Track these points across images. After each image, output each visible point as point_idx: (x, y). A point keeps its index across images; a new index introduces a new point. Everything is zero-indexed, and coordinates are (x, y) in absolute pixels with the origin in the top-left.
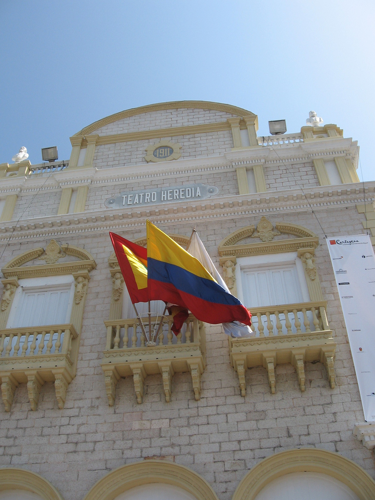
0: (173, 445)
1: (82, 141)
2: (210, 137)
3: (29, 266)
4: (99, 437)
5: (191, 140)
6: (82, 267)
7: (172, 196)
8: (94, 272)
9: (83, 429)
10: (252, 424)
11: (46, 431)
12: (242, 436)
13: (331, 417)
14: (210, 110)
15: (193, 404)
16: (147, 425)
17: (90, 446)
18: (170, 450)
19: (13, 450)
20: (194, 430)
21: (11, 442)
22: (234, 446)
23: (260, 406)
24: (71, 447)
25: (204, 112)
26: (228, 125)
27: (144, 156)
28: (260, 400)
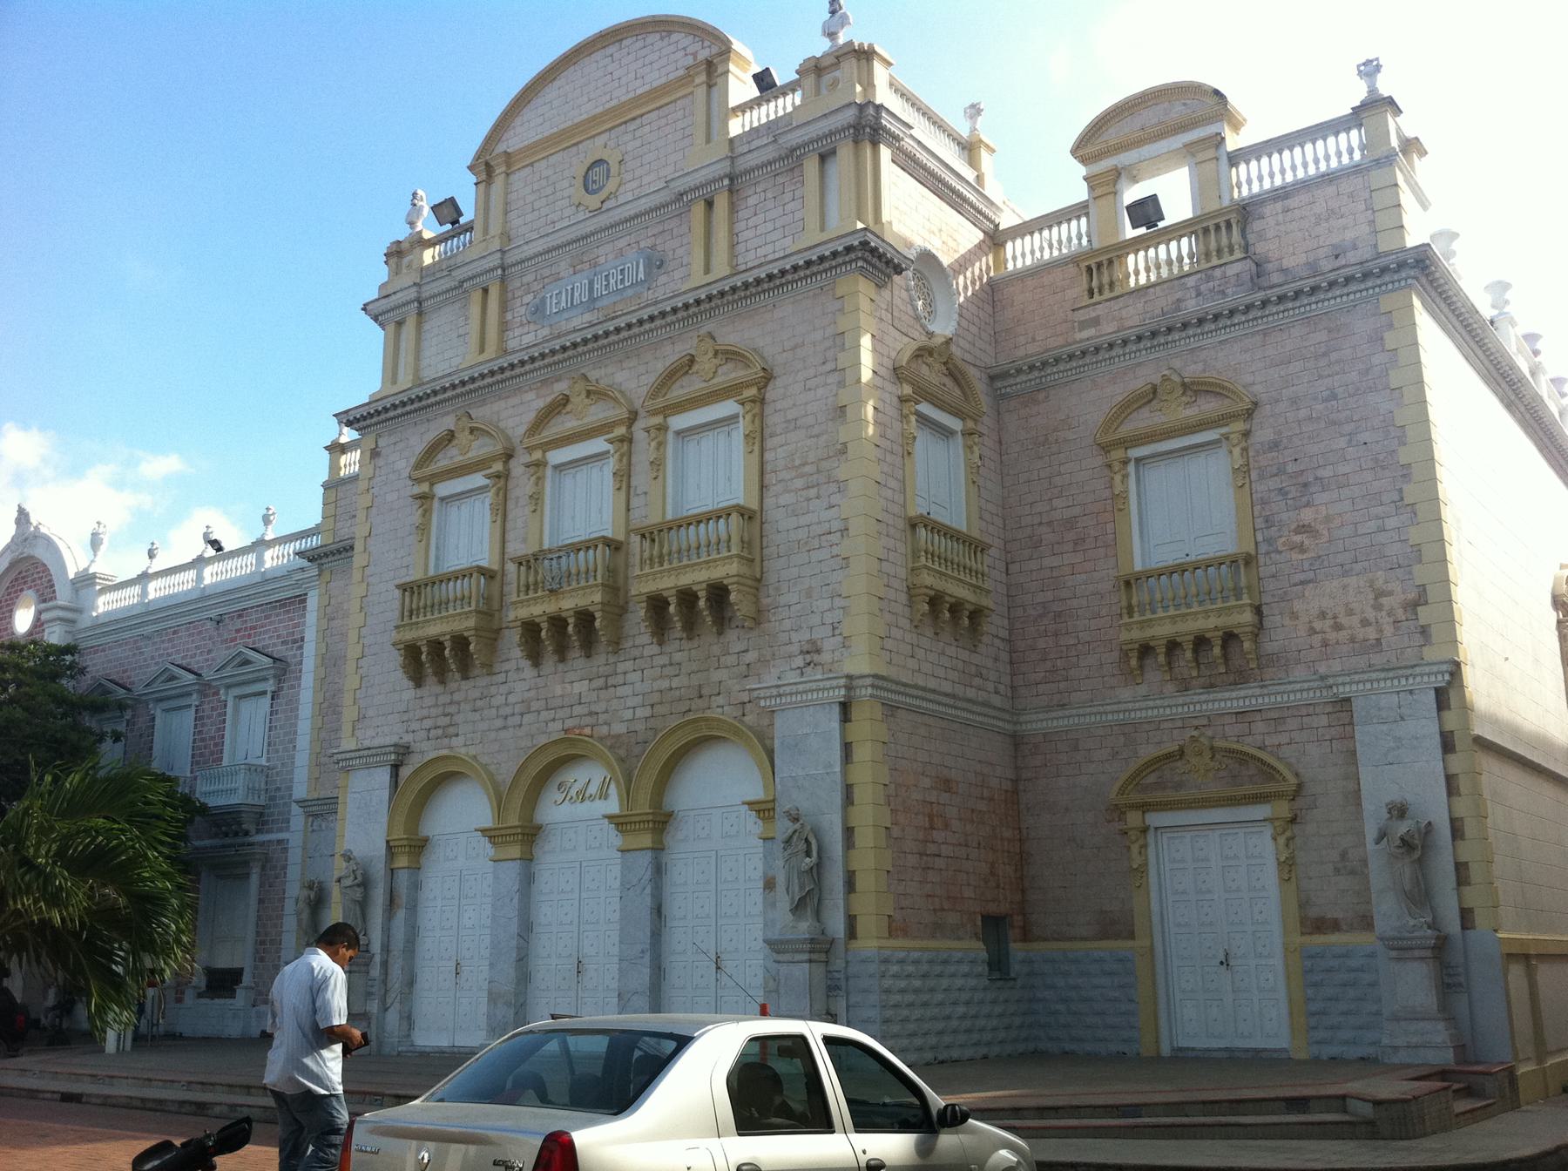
0: (591, 714)
1: (485, 167)
6: (493, 459)
8: (513, 463)
9: (511, 699)
14: (670, 33)
17: (517, 719)
18: (588, 720)
19: (451, 730)
21: (446, 720)
23: (678, 657)
25: (659, 44)
26: (687, 78)
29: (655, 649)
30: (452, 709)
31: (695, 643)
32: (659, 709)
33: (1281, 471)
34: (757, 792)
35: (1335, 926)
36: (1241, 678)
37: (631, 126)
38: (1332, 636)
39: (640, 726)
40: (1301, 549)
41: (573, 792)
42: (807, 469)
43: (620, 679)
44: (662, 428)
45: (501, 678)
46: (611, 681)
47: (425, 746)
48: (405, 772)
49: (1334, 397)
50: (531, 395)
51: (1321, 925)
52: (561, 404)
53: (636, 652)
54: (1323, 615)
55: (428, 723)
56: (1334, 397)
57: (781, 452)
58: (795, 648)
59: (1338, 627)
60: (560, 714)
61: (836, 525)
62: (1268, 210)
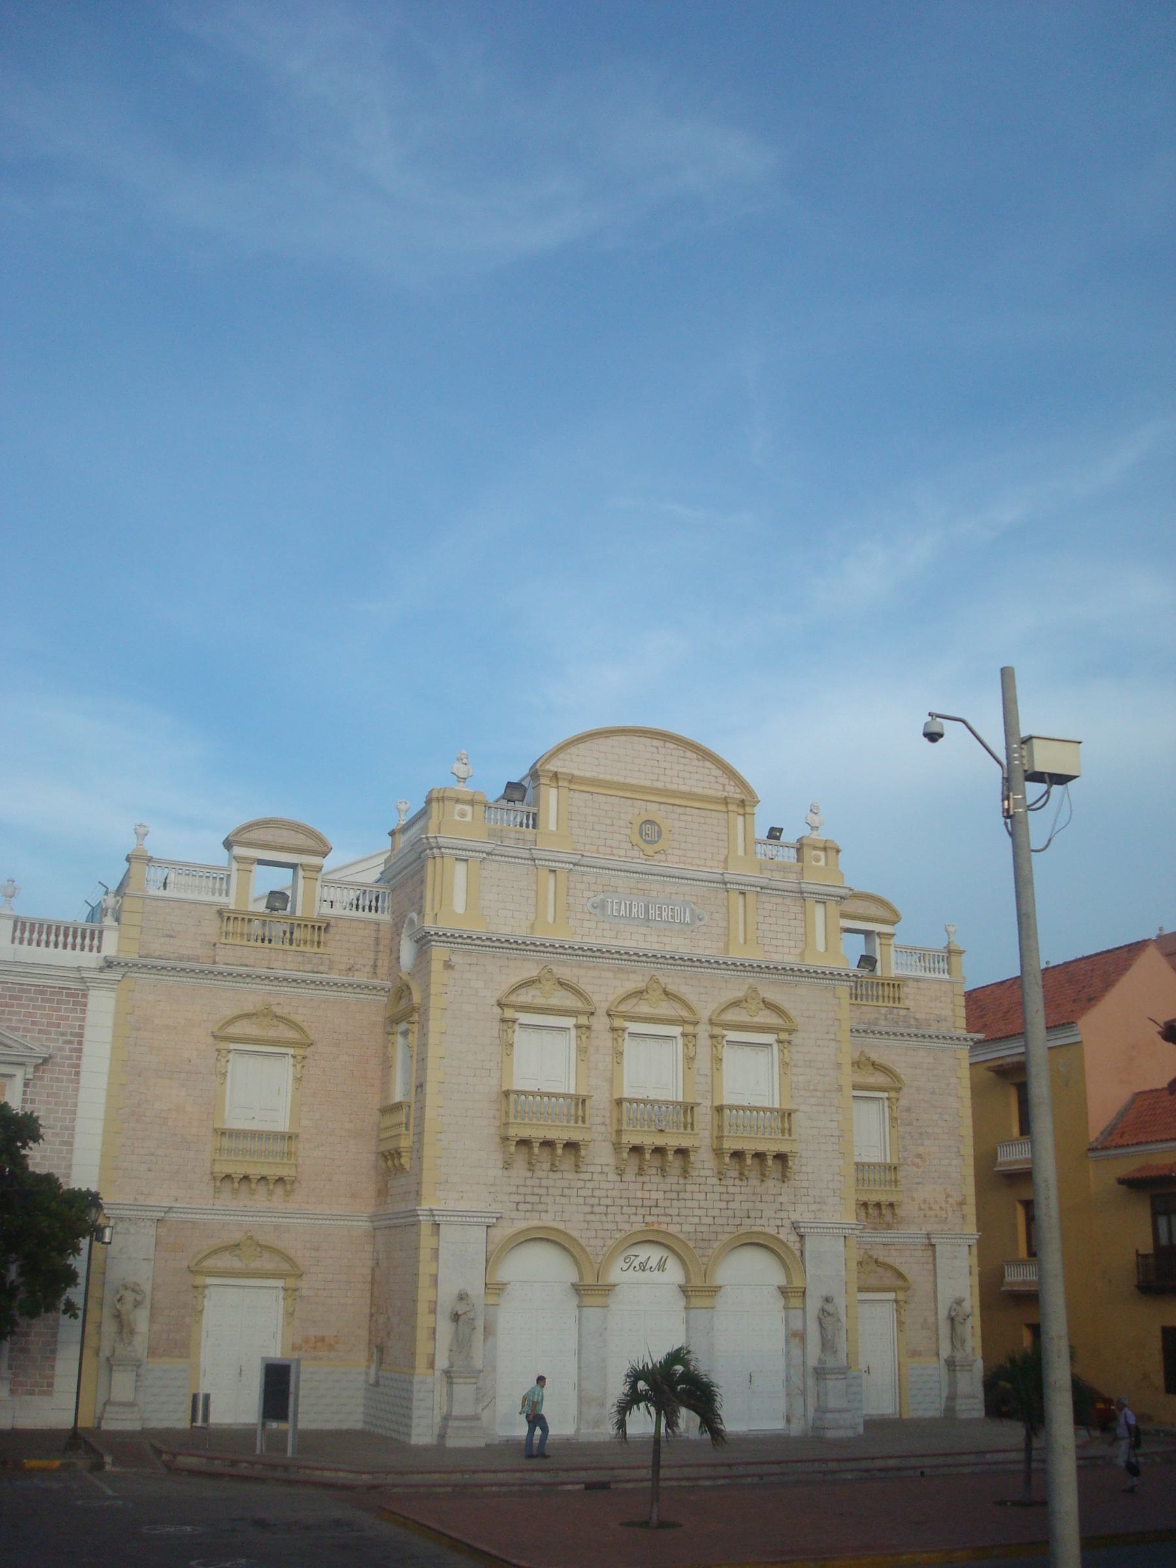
0: (666, 1215)
2: (702, 820)
3: (525, 997)
4: (609, 1201)
5: (682, 817)
7: (660, 915)
8: (593, 1020)
9: (597, 1193)
10: (723, 1205)
11: (566, 1191)
12: (716, 1213)
14: (704, 759)
15: (682, 1181)
16: (647, 1195)
17: (603, 1209)
19: (541, 1207)
21: (536, 1199)
22: (710, 1220)
23: (731, 1190)
25: (695, 762)
26: (725, 801)
27: (628, 831)
29: (715, 1181)
30: (543, 1191)
31: (744, 1183)
32: (718, 1221)
33: (910, 1124)
34: (781, 1280)
35: (920, 1354)
36: (889, 1227)
37: (679, 810)
38: (928, 1212)
39: (704, 1229)
40: (918, 1166)
41: (636, 1263)
42: (819, 1094)
43: (688, 1196)
44: (723, 1037)
45: (588, 1176)
46: (682, 1195)
47: (514, 1214)
49: (933, 1093)
50: (610, 975)
51: (914, 1354)
52: (639, 994)
53: (699, 1180)
54: (925, 1202)
55: (517, 1198)
56: (933, 1093)
59: (931, 1209)
61: (836, 1133)
62: (911, 984)
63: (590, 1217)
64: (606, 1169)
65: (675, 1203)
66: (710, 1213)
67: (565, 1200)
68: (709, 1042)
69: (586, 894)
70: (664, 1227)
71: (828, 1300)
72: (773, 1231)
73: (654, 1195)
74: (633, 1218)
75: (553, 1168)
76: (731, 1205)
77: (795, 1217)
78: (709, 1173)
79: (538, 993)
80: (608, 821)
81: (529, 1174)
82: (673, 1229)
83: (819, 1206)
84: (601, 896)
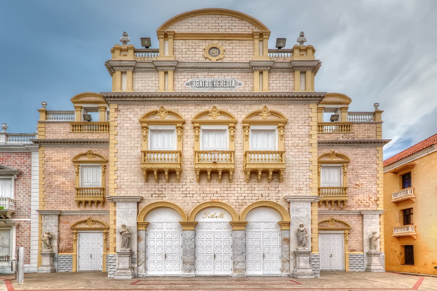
0: (221, 196)
2: (241, 45)
3: (153, 119)
4: (194, 192)
5: (231, 45)
6: (179, 122)
9: (188, 189)
11: (174, 189)
13: (277, 192)
15: (229, 183)
17: (192, 195)
18: (220, 198)
19: (162, 195)
20: (229, 192)
21: (161, 192)
22: (243, 198)
24: (184, 195)
28: (254, 184)
29: (246, 183)
30: (164, 190)
48: (143, 205)
57: (290, 142)
58: (294, 189)
60: (208, 195)
63: (185, 198)
64: (192, 181)
65: (225, 192)
66: (243, 195)
67: (174, 192)
68: (242, 130)
69: (183, 80)
70: (220, 201)
71: (301, 226)
72: (275, 201)
73: (215, 190)
74: (205, 198)
75: (168, 181)
76: (253, 192)
77: (285, 195)
78: (241, 180)
79: (159, 117)
80: (193, 50)
81: (157, 184)
82: (224, 201)
83: (298, 191)
84: (191, 80)
